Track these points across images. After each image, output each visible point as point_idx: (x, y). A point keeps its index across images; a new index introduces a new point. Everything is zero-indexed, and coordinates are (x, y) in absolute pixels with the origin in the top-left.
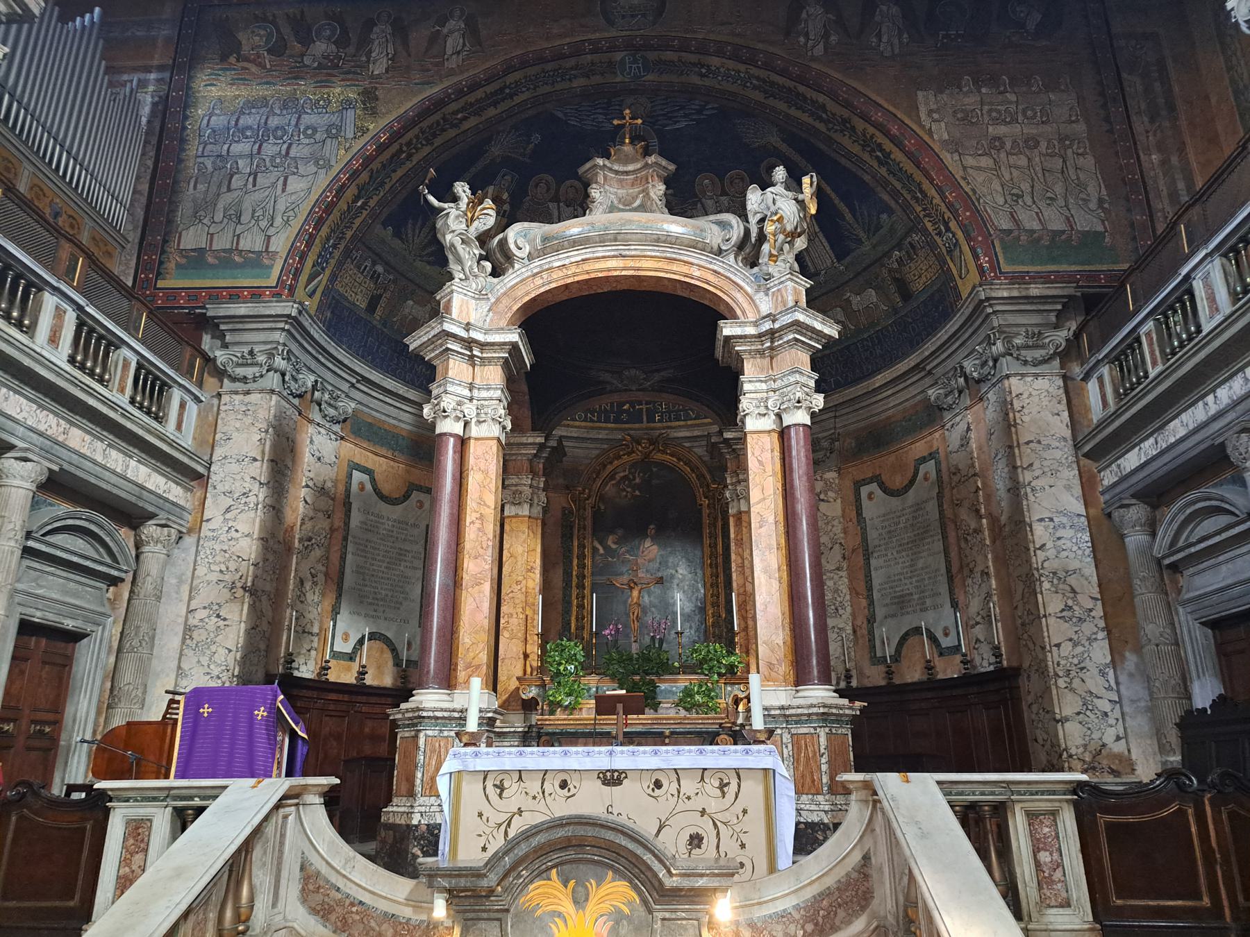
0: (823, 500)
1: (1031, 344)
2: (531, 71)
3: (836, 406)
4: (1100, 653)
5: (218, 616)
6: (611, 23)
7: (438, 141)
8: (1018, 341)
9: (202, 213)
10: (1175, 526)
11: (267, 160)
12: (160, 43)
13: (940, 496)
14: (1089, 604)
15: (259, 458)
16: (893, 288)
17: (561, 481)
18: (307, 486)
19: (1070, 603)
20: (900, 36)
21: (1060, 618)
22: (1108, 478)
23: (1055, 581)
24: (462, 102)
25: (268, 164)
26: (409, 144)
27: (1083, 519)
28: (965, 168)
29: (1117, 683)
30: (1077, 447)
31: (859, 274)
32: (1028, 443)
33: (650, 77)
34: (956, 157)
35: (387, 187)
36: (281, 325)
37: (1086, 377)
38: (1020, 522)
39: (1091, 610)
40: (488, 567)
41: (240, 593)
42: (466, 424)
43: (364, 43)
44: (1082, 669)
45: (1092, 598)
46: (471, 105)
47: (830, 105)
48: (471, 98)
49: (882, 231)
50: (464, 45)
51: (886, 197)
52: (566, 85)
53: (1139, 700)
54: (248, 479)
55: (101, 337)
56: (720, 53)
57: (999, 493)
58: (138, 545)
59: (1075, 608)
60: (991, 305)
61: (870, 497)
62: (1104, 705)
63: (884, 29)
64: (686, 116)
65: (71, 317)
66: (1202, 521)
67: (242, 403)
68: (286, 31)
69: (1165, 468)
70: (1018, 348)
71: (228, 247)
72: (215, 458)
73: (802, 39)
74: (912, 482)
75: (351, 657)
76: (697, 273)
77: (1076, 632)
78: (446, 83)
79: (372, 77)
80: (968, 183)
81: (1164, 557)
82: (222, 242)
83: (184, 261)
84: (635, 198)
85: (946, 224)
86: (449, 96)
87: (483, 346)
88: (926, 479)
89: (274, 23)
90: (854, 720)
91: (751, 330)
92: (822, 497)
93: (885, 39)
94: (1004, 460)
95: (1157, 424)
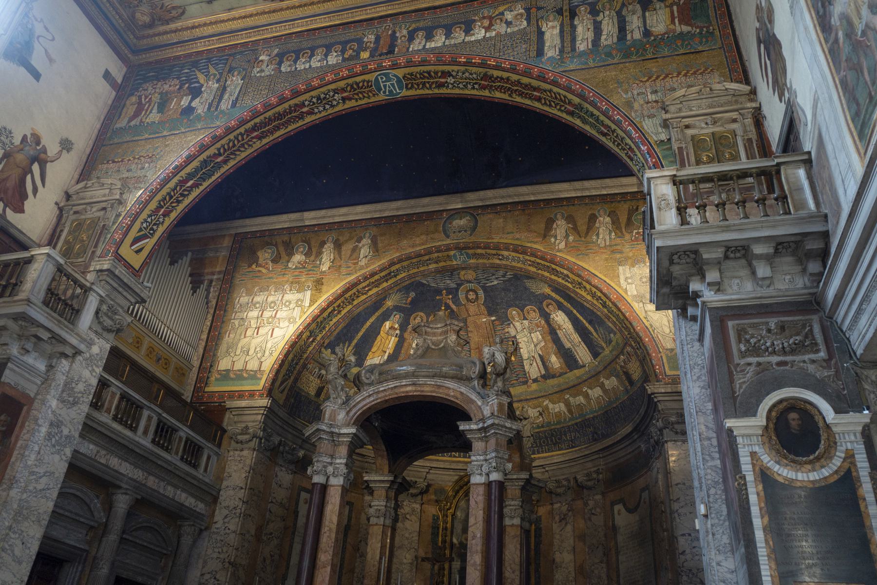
0: (593, 514)
1: (680, 421)
2: (405, 264)
3: (599, 450)
5: (215, 578)
6: (448, 237)
7: (355, 303)
8: (672, 419)
9: (231, 350)
11: (265, 319)
12: (221, 259)
15: (244, 487)
16: (624, 377)
17: (433, 497)
18: (272, 502)
20: (610, 234)
23: (691, 575)
24: (367, 282)
25: (265, 322)
26: (339, 306)
28: (646, 312)
31: (605, 368)
32: (677, 485)
33: (472, 261)
34: (641, 305)
35: (327, 329)
36: (262, 412)
40: (330, 558)
41: (227, 565)
42: (328, 478)
43: (319, 253)
46: (373, 283)
47: (571, 275)
48: (372, 280)
49: (613, 343)
50: (369, 252)
51: (610, 325)
52: (425, 268)
54: (237, 499)
55: (169, 427)
56: (507, 249)
58: (179, 537)
60: (655, 397)
61: (619, 514)
63: (601, 231)
64: (497, 278)
65: (155, 419)
67: (239, 456)
68: (281, 249)
70: (673, 424)
71: (241, 368)
72: (223, 487)
73: (553, 240)
76: (452, 394)
78: (359, 274)
79: (322, 272)
80: (648, 321)
82: (238, 366)
83: (219, 376)
84: (441, 342)
85: (639, 344)
86: (360, 280)
88: (645, 503)
89: (276, 245)
91: (474, 427)
92: (593, 511)
93: (601, 236)
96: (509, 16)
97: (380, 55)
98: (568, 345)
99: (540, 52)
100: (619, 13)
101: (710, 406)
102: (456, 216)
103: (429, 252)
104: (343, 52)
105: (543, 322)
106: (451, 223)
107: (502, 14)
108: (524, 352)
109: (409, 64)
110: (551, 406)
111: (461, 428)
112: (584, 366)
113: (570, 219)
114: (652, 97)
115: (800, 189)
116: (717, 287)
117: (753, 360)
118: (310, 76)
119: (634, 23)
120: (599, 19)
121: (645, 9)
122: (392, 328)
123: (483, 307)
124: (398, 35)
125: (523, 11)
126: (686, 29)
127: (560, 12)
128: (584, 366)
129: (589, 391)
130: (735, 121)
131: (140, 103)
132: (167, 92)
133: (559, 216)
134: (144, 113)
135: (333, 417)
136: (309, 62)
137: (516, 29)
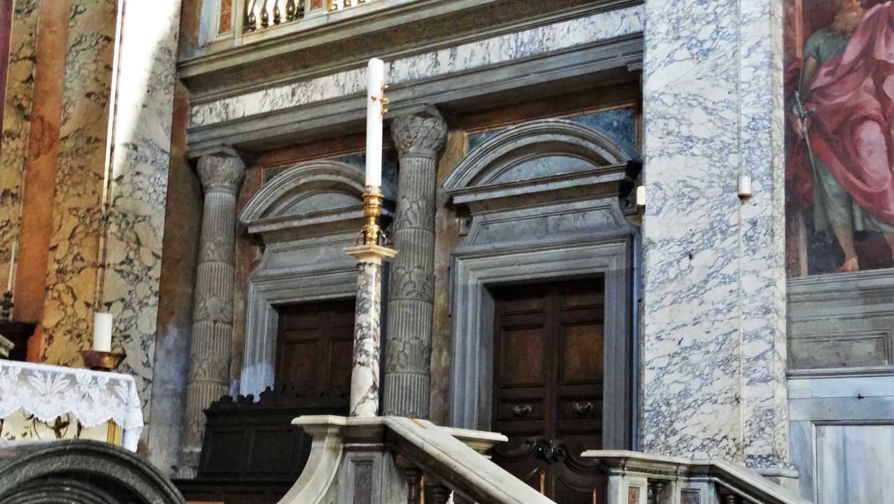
10: (279, 193)
19: (132, 255)
21: (118, 271)
23: (123, 225)
27: (166, 157)
29: (155, 360)
38: (97, 140)
39: (149, 269)
44: (126, 337)
45: (154, 254)
53: (167, 382)
57: (69, 93)
59: (136, 262)
66: (312, 194)
69: (297, 126)
77: (130, 292)
81: (251, 224)
94: (92, 54)
95: (302, 73)
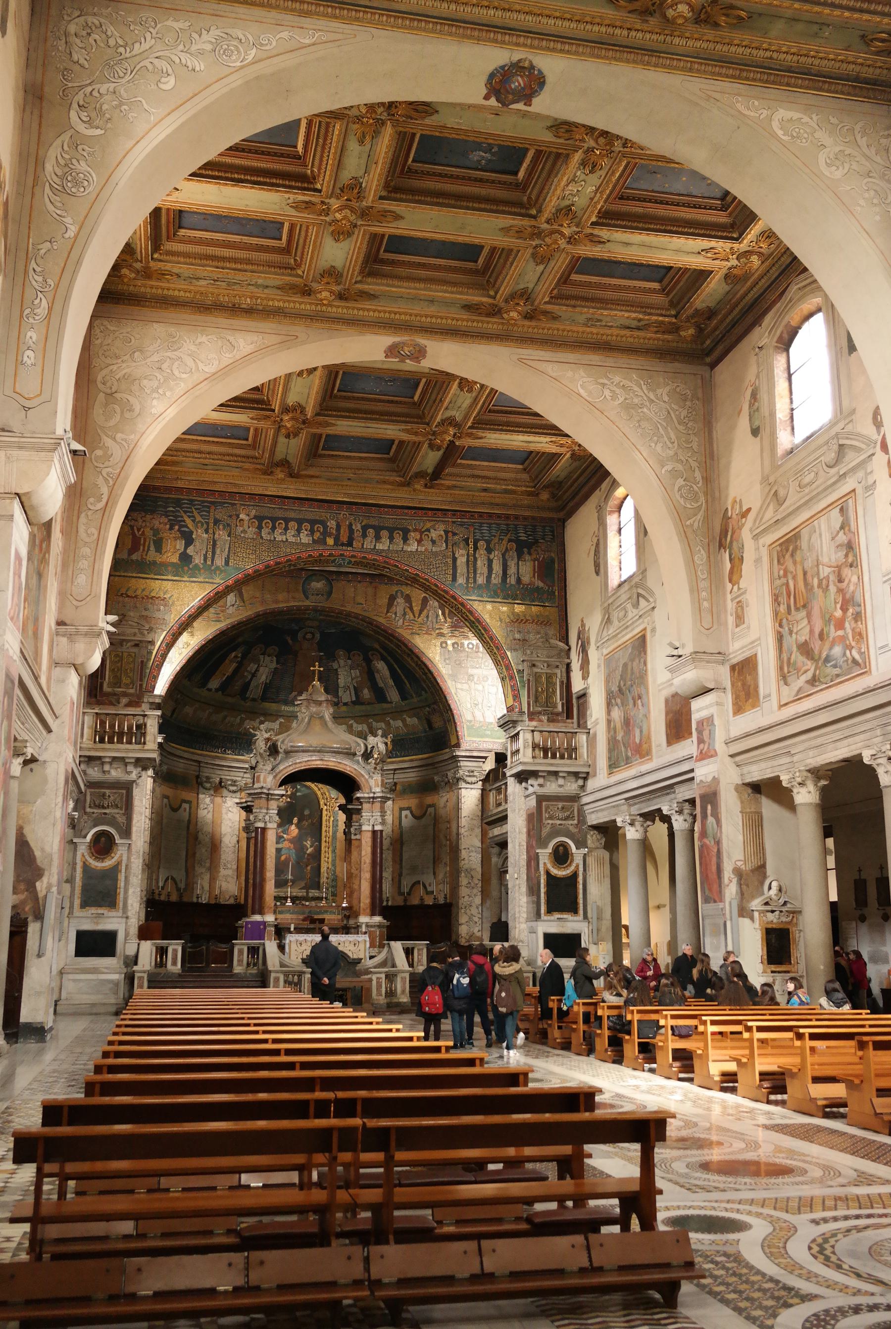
4: (478, 900)
6: (307, 598)
13: (435, 825)
14: (477, 882)
16: (425, 722)
22: (491, 835)
30: (482, 820)
37: (490, 791)
61: (406, 816)
62: (476, 919)
74: (425, 814)
75: (163, 888)
87: (272, 795)
90: (388, 927)
91: (366, 795)
93: (430, 619)
95: (500, 823)
96: (434, 534)
97: (343, 545)
98: (381, 685)
99: (454, 579)
100: (504, 555)
101: (525, 830)
102: (314, 578)
103: (289, 610)
104: (312, 532)
105: (364, 664)
106: (309, 584)
107: (428, 530)
108: (341, 682)
109: (364, 558)
110: (355, 725)
111: (358, 795)
112: (391, 703)
113: (408, 598)
114: (517, 636)
115: (583, 746)
116: (541, 786)
117: (550, 822)
118: (288, 550)
119: (512, 570)
120: (492, 556)
121: (519, 559)
122: (236, 657)
123: (315, 645)
124: (354, 527)
125: (443, 533)
126: (541, 584)
127: (466, 541)
128: (391, 703)
129: (391, 721)
130: (557, 667)
131: (133, 534)
132: (158, 529)
133: (399, 594)
134: (142, 548)
135: (265, 782)
136: (285, 534)
137: (438, 549)
